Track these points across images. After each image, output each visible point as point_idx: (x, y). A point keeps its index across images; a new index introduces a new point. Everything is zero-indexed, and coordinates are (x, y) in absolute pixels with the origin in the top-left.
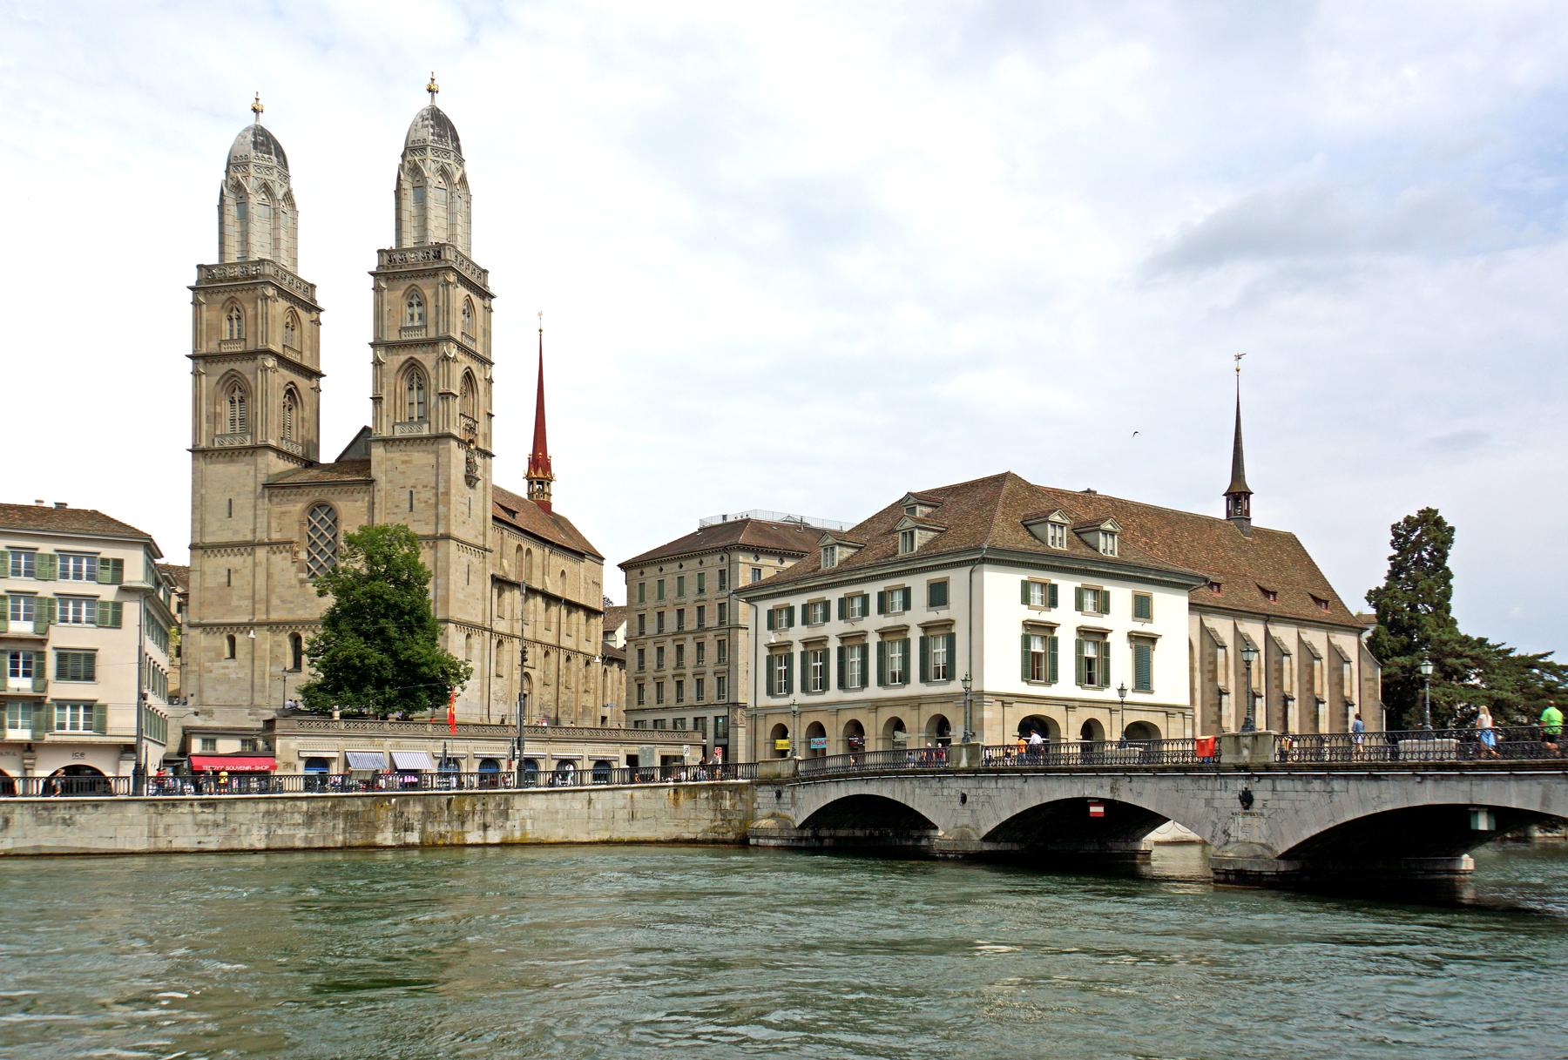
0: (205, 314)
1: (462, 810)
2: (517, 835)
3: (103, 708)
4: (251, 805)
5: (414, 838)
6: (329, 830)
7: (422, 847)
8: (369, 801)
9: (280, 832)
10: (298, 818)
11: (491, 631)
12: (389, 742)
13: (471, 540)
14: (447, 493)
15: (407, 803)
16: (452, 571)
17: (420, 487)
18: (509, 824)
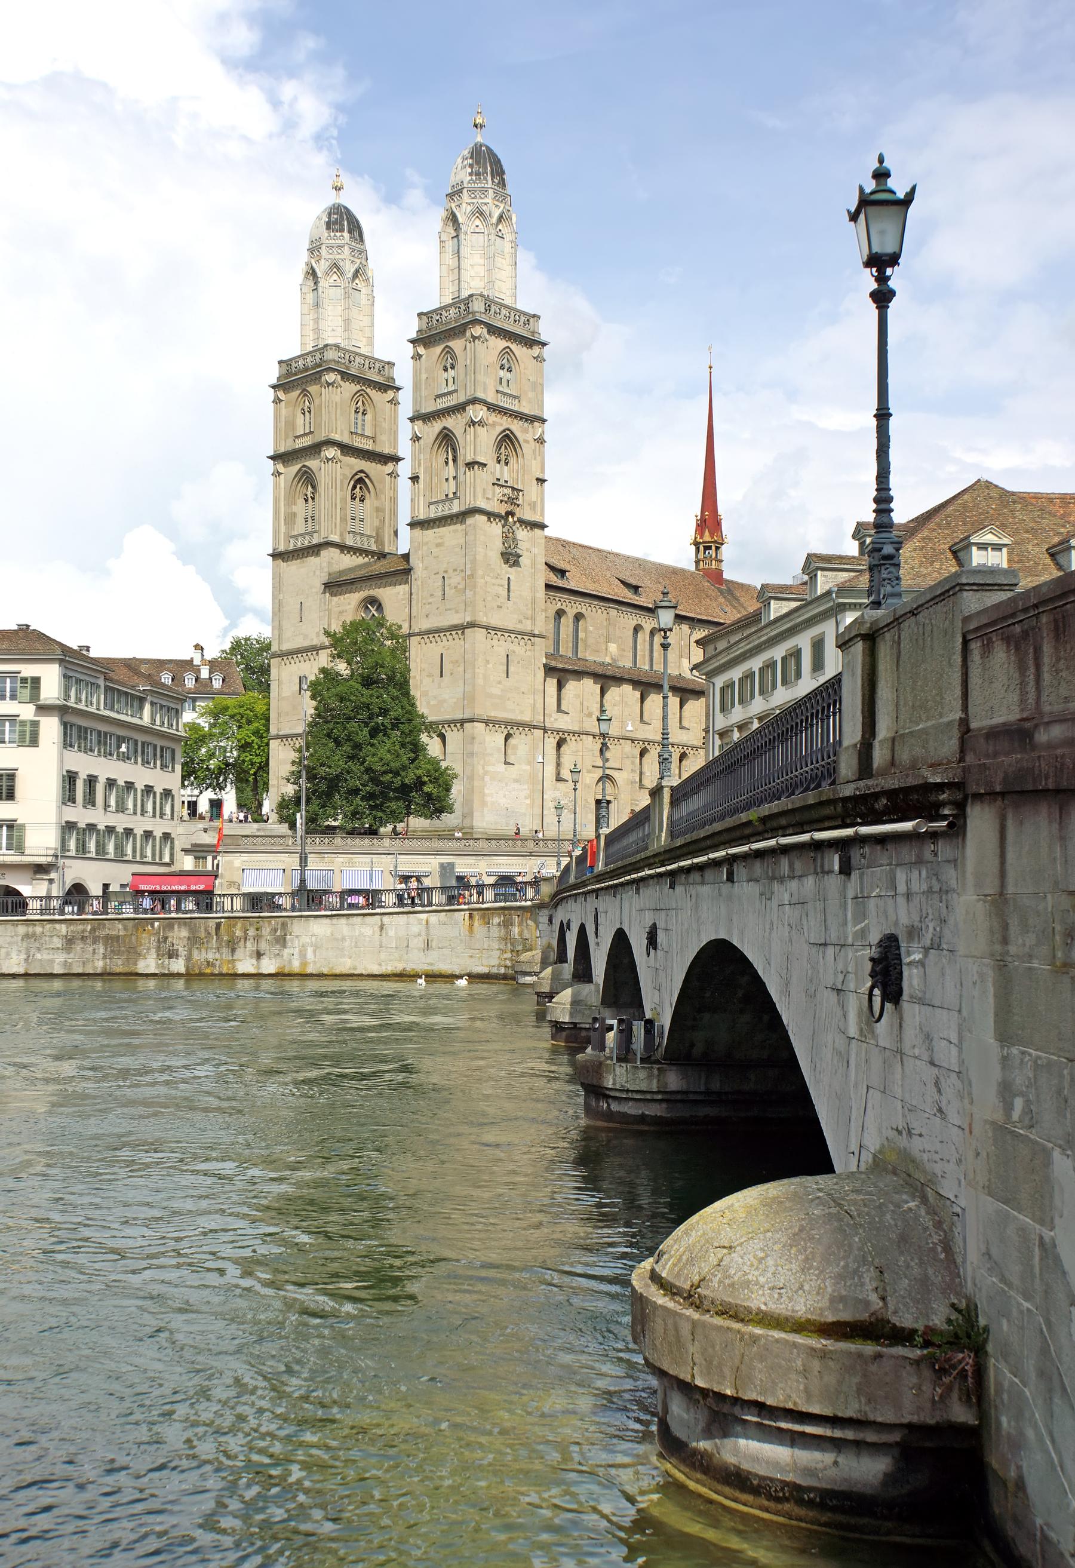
0: (284, 412)
1: (232, 935)
2: (296, 966)
3: (22, 827)
4: (10, 927)
5: (178, 966)
6: (89, 956)
7: (189, 976)
8: (131, 924)
9: (39, 956)
10: (57, 942)
11: (545, 730)
12: (341, 858)
13: (511, 626)
14: (472, 576)
15: (171, 927)
17: (450, 571)
18: (286, 952)
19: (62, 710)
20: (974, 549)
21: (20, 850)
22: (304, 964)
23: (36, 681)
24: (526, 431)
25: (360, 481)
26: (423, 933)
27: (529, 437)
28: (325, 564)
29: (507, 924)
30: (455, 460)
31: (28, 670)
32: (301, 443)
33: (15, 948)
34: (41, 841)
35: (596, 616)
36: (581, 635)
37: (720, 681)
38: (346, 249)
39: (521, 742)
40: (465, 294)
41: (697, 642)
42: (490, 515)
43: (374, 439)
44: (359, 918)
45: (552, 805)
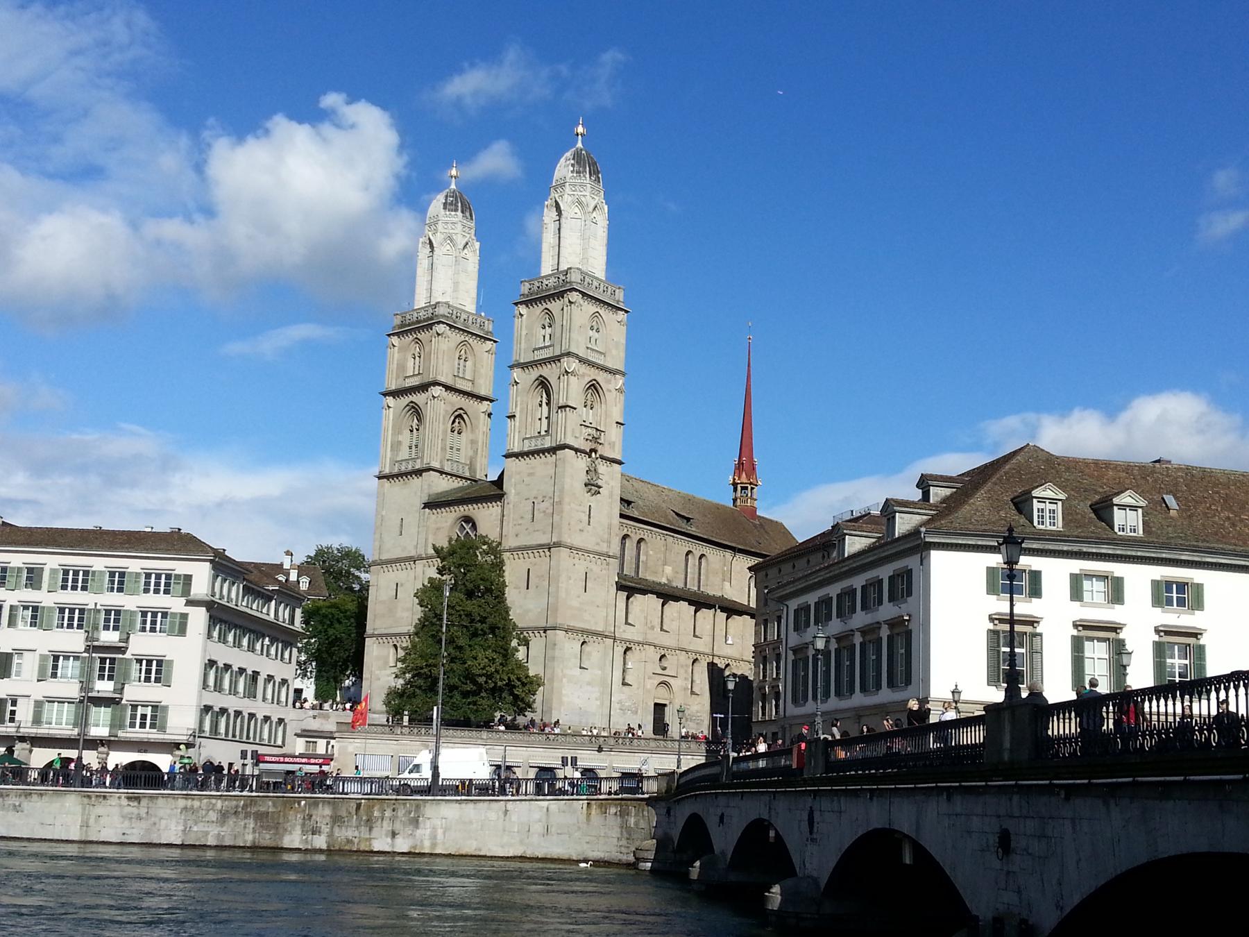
3: (165, 708)
9: (195, 829)
10: (213, 816)
14: (560, 503)
16: (563, 578)
18: (419, 832)
19: (210, 605)
20: (1035, 501)
21: (163, 729)
22: (434, 845)
23: (188, 579)
24: (609, 382)
25: (459, 416)
26: (544, 820)
27: (611, 387)
28: (425, 487)
29: (623, 814)
30: (548, 404)
31: (181, 568)
32: (410, 383)
33: (174, 821)
34: (181, 722)
35: (656, 543)
36: (642, 558)
37: (793, 604)
38: (459, 226)
39: (596, 650)
40: (563, 267)
41: (750, 569)
42: (576, 450)
43: (473, 382)
44: (486, 804)
45: (618, 706)
